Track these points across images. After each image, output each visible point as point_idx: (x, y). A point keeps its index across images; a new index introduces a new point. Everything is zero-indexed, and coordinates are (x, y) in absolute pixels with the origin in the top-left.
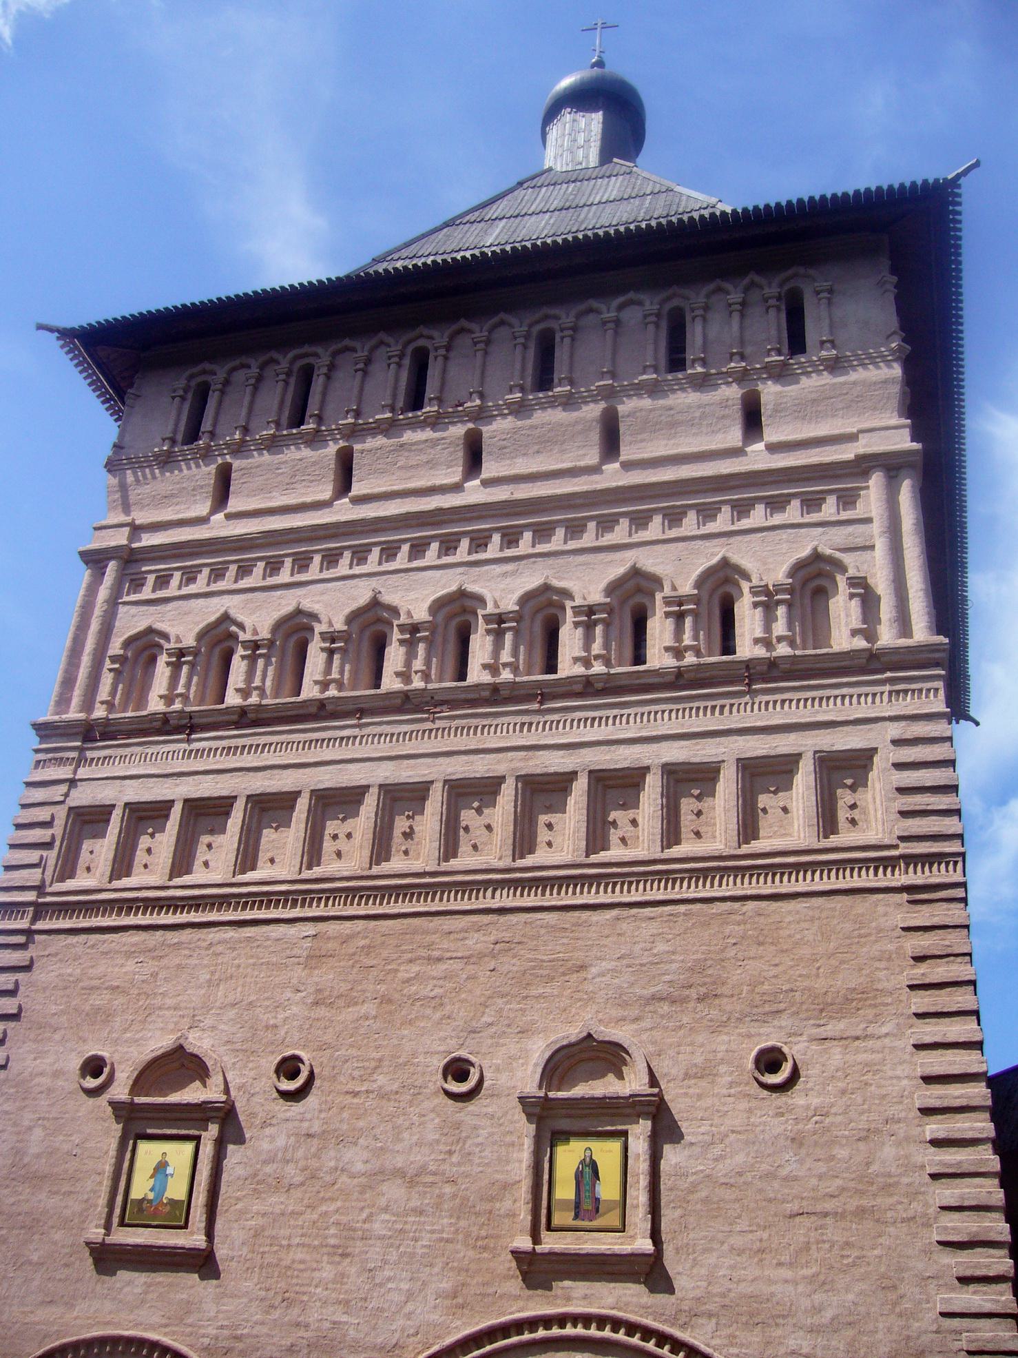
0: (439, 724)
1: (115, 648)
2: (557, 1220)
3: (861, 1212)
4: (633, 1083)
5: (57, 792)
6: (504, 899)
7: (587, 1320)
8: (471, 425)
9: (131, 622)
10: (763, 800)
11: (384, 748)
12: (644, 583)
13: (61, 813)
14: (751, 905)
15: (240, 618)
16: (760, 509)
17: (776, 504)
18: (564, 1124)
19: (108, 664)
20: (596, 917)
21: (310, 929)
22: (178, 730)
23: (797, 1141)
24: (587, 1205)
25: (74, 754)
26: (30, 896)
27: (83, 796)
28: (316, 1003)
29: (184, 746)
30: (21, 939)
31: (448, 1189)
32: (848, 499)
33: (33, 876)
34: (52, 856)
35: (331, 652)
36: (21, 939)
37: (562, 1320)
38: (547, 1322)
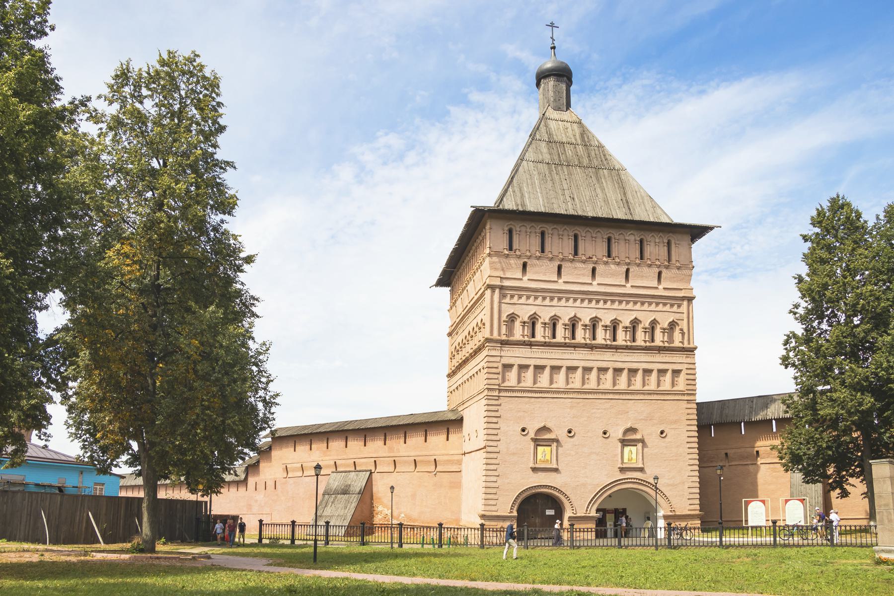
0: (594, 352)
1: (504, 318)
2: (625, 462)
3: (676, 460)
4: (638, 436)
5: (498, 359)
6: (611, 396)
7: (632, 478)
8: (593, 265)
9: (507, 310)
10: (661, 378)
11: (581, 357)
12: (637, 321)
13: (500, 366)
14: (659, 401)
15: (540, 315)
16: (661, 305)
17: (665, 304)
18: (626, 443)
19: (503, 323)
20: (630, 401)
21: (570, 400)
22: (527, 345)
23: (666, 447)
24: (630, 458)
25: (499, 348)
26: (497, 387)
27: (506, 361)
28: (573, 417)
29: (529, 350)
30: (497, 398)
31: (605, 456)
32: (679, 306)
33: (496, 382)
34: (500, 377)
35: (565, 329)
36: (497, 398)
37: (627, 479)
38: (625, 479)
